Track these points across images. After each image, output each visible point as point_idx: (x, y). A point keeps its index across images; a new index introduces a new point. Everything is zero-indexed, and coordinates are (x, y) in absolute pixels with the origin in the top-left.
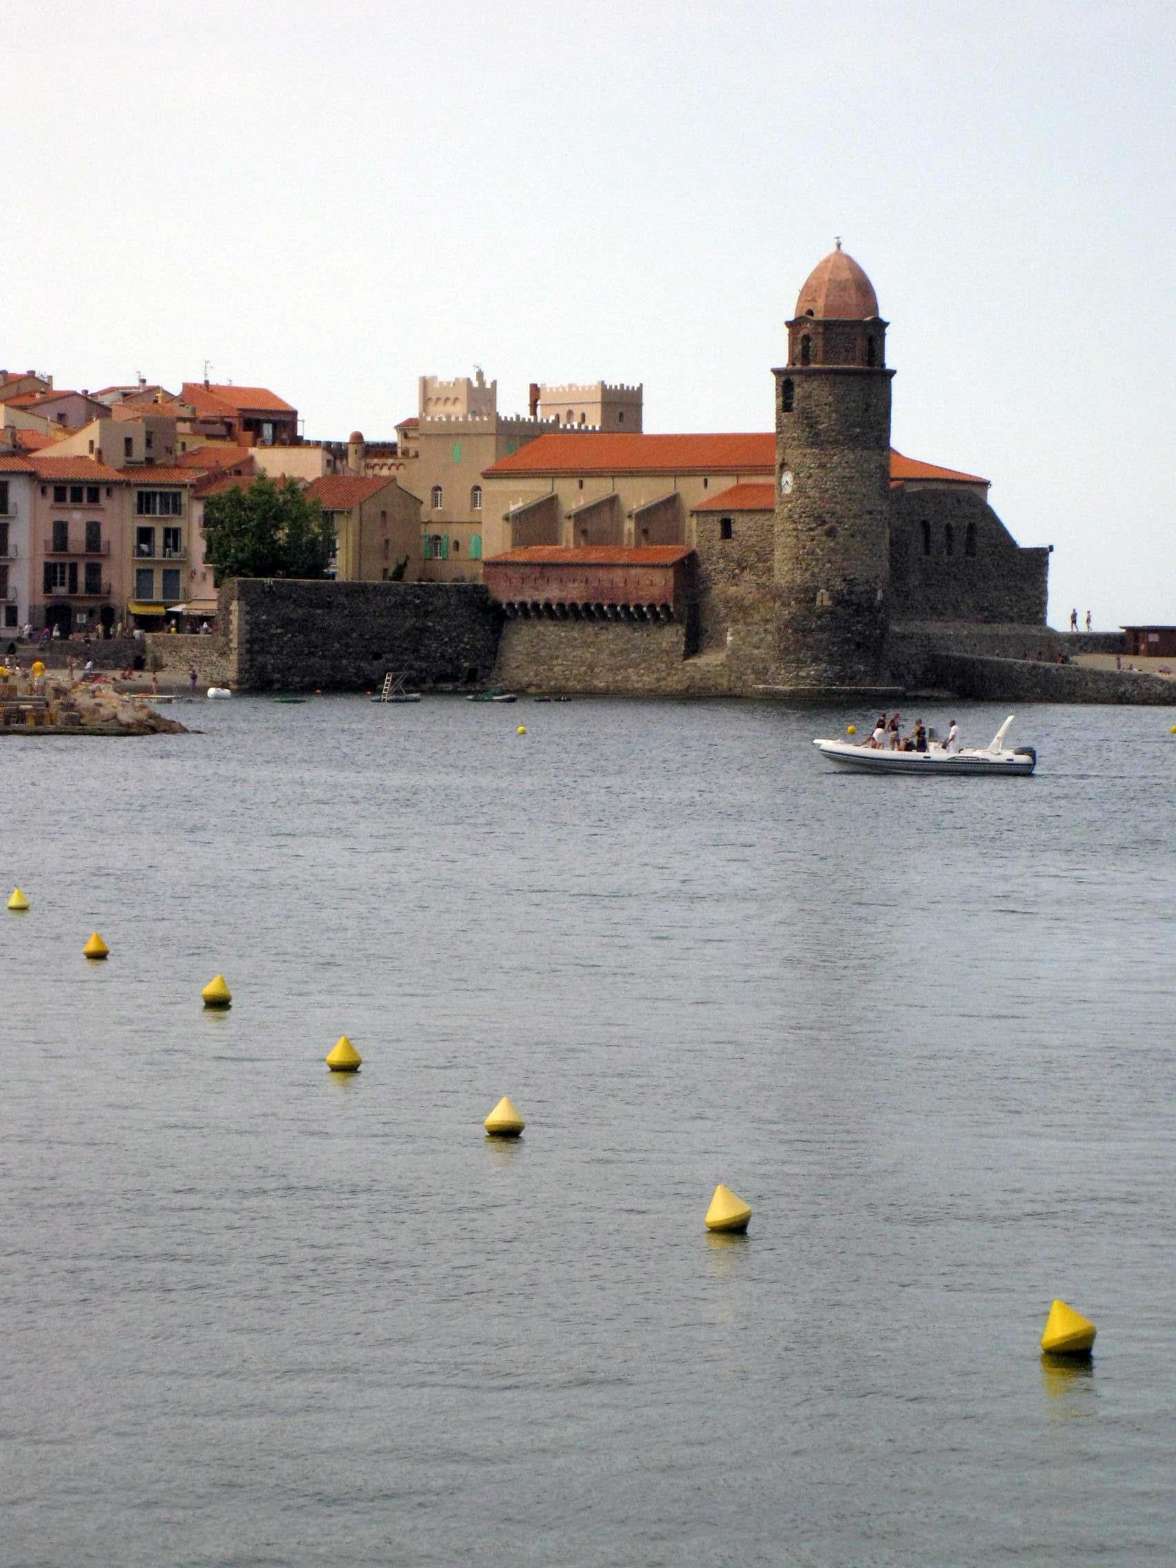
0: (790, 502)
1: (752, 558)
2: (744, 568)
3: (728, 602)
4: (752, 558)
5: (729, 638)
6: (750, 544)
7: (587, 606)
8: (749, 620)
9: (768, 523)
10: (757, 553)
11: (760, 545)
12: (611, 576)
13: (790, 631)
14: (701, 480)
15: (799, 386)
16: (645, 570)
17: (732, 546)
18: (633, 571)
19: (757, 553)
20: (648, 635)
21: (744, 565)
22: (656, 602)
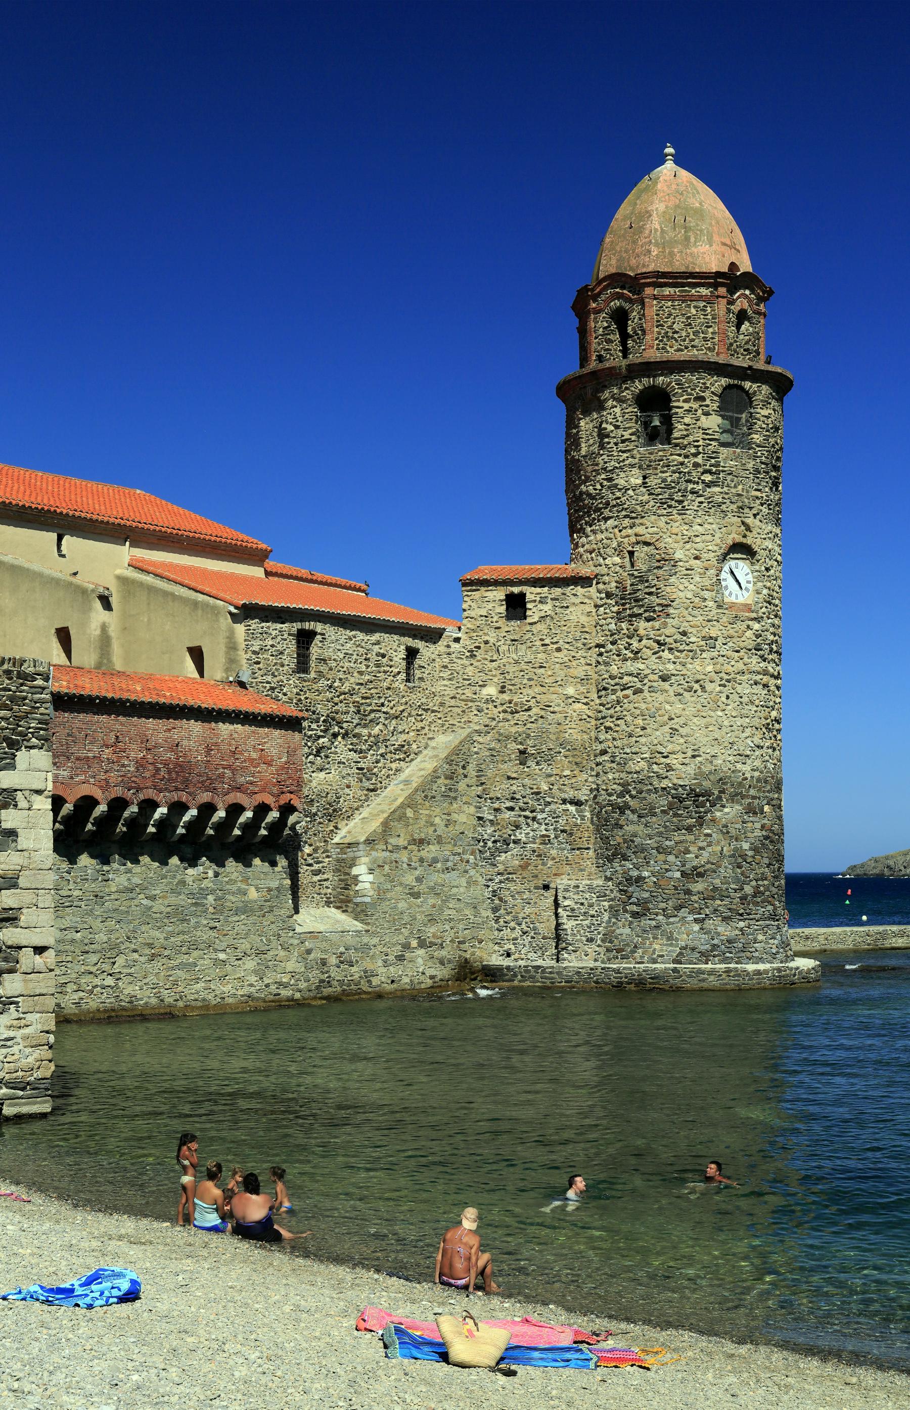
2: (335, 735)
4: (350, 719)
6: (346, 687)
8: (393, 841)
9: (376, 648)
10: (358, 705)
12: (176, 735)
15: (766, 404)
18: (225, 729)
19: (358, 705)
20: (216, 875)
21: (336, 729)
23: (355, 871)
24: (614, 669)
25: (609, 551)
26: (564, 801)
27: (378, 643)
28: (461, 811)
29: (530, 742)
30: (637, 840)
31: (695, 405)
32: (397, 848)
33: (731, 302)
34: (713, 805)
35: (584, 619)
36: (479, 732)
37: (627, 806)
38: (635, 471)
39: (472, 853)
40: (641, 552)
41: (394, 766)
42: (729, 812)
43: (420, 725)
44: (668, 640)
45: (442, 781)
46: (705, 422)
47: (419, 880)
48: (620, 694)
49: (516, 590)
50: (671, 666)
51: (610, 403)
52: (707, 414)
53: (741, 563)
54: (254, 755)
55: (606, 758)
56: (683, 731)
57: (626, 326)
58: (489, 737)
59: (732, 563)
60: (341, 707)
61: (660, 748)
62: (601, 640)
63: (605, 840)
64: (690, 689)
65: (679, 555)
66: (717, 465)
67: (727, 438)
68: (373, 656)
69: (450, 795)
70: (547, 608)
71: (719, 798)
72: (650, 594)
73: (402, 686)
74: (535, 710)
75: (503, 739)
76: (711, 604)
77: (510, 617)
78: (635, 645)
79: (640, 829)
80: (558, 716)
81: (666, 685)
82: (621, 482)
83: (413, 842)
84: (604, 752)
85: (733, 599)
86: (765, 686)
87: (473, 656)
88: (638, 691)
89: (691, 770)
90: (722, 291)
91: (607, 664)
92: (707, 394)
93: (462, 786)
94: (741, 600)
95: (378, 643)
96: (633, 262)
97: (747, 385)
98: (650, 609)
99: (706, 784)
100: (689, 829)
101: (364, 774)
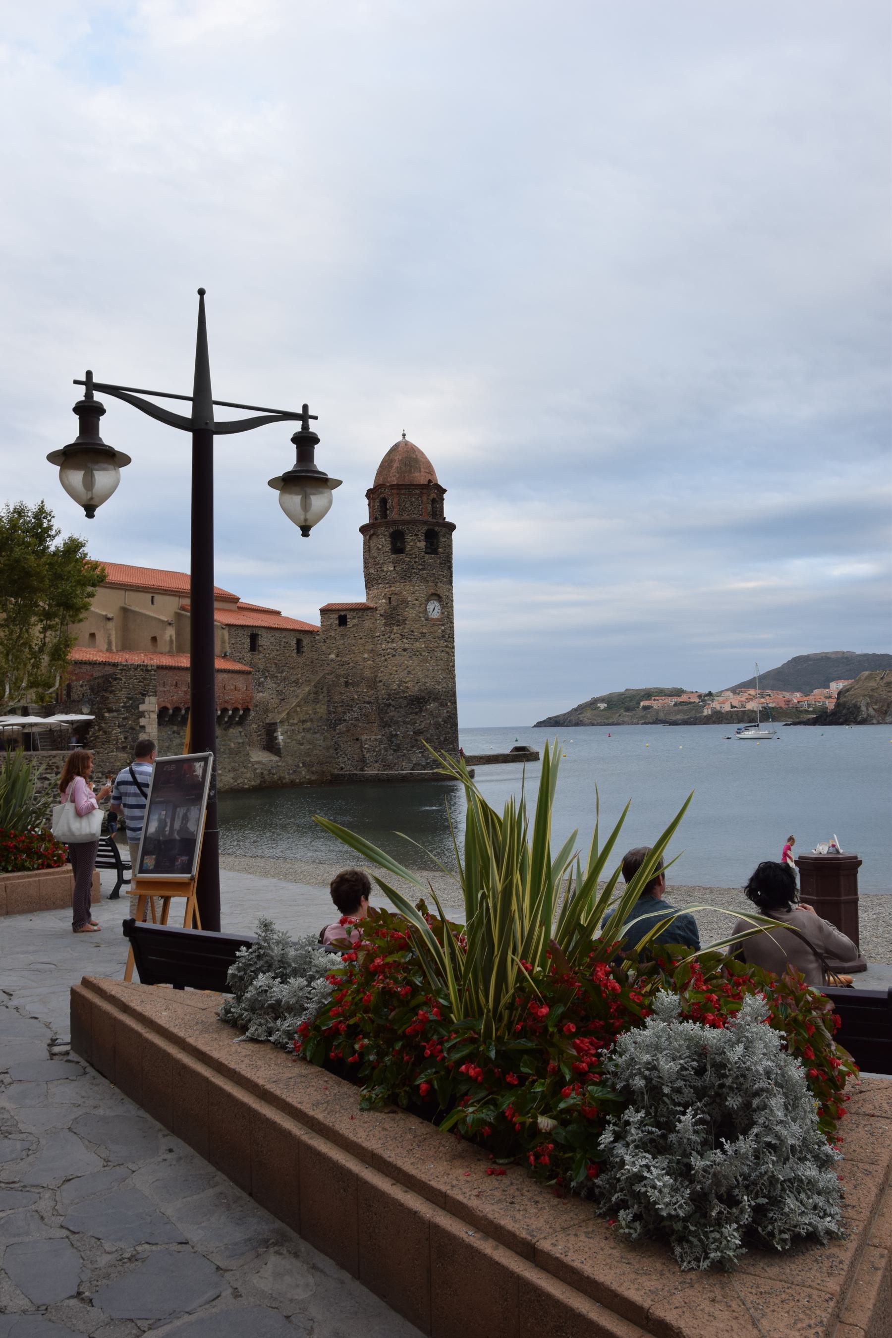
0: (443, 625)
1: (273, 669)
2: (266, 677)
3: (256, 706)
5: (281, 737)
7: (177, 709)
8: (291, 721)
9: (284, 640)
10: (276, 664)
11: (278, 658)
13: (449, 726)
14: (150, 596)
15: (444, 536)
16: (230, 675)
17: (259, 659)
19: (276, 664)
22: (239, 706)
23: (275, 735)
24: (384, 646)
25: (381, 597)
26: (364, 702)
27: (284, 637)
28: (320, 708)
29: (350, 678)
30: (395, 719)
31: (414, 538)
32: (293, 724)
33: (429, 495)
34: (426, 703)
35: (371, 626)
36: (328, 674)
37: (390, 704)
38: (391, 564)
39: (326, 725)
40: (394, 598)
41: (292, 689)
42: (432, 706)
43: (303, 671)
44: (406, 634)
45: (312, 695)
46: (418, 544)
47: (303, 738)
48: (387, 657)
49: (342, 613)
50: (407, 645)
51: (380, 536)
52: (419, 541)
53: (435, 602)
54: (232, 687)
55: (381, 684)
56: (413, 672)
57: (386, 505)
58: (332, 676)
59: (432, 602)
60: (268, 665)
61: (403, 680)
62: (378, 634)
63: (382, 719)
64: (415, 655)
65: (409, 599)
66: (424, 562)
67: (429, 550)
68: (283, 644)
69: (316, 701)
70: (355, 621)
71: (428, 700)
72: (398, 615)
73: (295, 655)
74: (351, 664)
75: (338, 676)
76: (423, 619)
77: (340, 625)
78: (392, 636)
79: (395, 714)
80: (361, 667)
81: (405, 653)
82: (385, 569)
83: (300, 721)
84: (381, 681)
85: (432, 616)
86: (447, 653)
87: (325, 641)
88: (394, 656)
89: (416, 688)
90: (425, 491)
91: (381, 644)
92: (419, 533)
93: (321, 697)
94: (436, 617)
95: (284, 637)
96: (389, 479)
97: (436, 529)
98: (399, 621)
99: (423, 694)
100: (416, 713)
101: (279, 693)
